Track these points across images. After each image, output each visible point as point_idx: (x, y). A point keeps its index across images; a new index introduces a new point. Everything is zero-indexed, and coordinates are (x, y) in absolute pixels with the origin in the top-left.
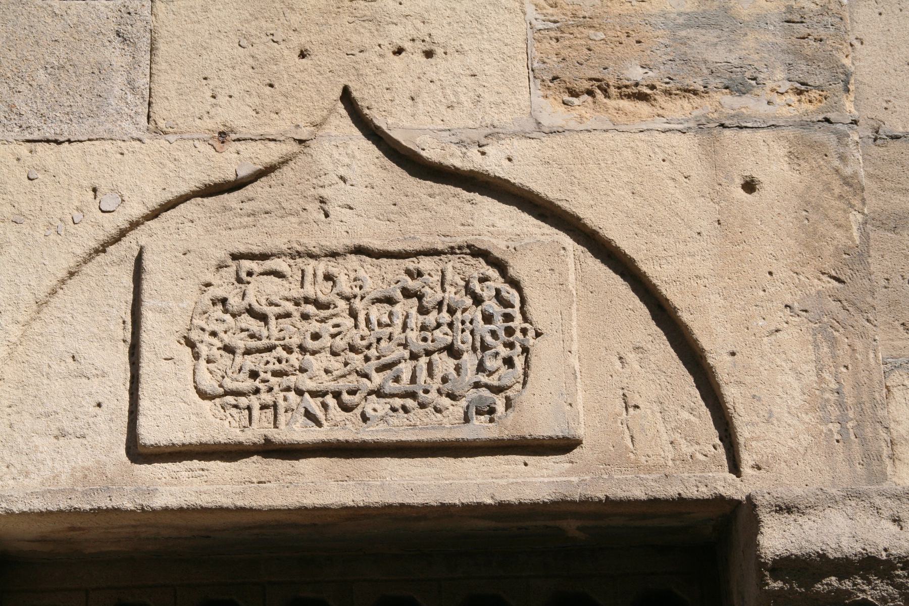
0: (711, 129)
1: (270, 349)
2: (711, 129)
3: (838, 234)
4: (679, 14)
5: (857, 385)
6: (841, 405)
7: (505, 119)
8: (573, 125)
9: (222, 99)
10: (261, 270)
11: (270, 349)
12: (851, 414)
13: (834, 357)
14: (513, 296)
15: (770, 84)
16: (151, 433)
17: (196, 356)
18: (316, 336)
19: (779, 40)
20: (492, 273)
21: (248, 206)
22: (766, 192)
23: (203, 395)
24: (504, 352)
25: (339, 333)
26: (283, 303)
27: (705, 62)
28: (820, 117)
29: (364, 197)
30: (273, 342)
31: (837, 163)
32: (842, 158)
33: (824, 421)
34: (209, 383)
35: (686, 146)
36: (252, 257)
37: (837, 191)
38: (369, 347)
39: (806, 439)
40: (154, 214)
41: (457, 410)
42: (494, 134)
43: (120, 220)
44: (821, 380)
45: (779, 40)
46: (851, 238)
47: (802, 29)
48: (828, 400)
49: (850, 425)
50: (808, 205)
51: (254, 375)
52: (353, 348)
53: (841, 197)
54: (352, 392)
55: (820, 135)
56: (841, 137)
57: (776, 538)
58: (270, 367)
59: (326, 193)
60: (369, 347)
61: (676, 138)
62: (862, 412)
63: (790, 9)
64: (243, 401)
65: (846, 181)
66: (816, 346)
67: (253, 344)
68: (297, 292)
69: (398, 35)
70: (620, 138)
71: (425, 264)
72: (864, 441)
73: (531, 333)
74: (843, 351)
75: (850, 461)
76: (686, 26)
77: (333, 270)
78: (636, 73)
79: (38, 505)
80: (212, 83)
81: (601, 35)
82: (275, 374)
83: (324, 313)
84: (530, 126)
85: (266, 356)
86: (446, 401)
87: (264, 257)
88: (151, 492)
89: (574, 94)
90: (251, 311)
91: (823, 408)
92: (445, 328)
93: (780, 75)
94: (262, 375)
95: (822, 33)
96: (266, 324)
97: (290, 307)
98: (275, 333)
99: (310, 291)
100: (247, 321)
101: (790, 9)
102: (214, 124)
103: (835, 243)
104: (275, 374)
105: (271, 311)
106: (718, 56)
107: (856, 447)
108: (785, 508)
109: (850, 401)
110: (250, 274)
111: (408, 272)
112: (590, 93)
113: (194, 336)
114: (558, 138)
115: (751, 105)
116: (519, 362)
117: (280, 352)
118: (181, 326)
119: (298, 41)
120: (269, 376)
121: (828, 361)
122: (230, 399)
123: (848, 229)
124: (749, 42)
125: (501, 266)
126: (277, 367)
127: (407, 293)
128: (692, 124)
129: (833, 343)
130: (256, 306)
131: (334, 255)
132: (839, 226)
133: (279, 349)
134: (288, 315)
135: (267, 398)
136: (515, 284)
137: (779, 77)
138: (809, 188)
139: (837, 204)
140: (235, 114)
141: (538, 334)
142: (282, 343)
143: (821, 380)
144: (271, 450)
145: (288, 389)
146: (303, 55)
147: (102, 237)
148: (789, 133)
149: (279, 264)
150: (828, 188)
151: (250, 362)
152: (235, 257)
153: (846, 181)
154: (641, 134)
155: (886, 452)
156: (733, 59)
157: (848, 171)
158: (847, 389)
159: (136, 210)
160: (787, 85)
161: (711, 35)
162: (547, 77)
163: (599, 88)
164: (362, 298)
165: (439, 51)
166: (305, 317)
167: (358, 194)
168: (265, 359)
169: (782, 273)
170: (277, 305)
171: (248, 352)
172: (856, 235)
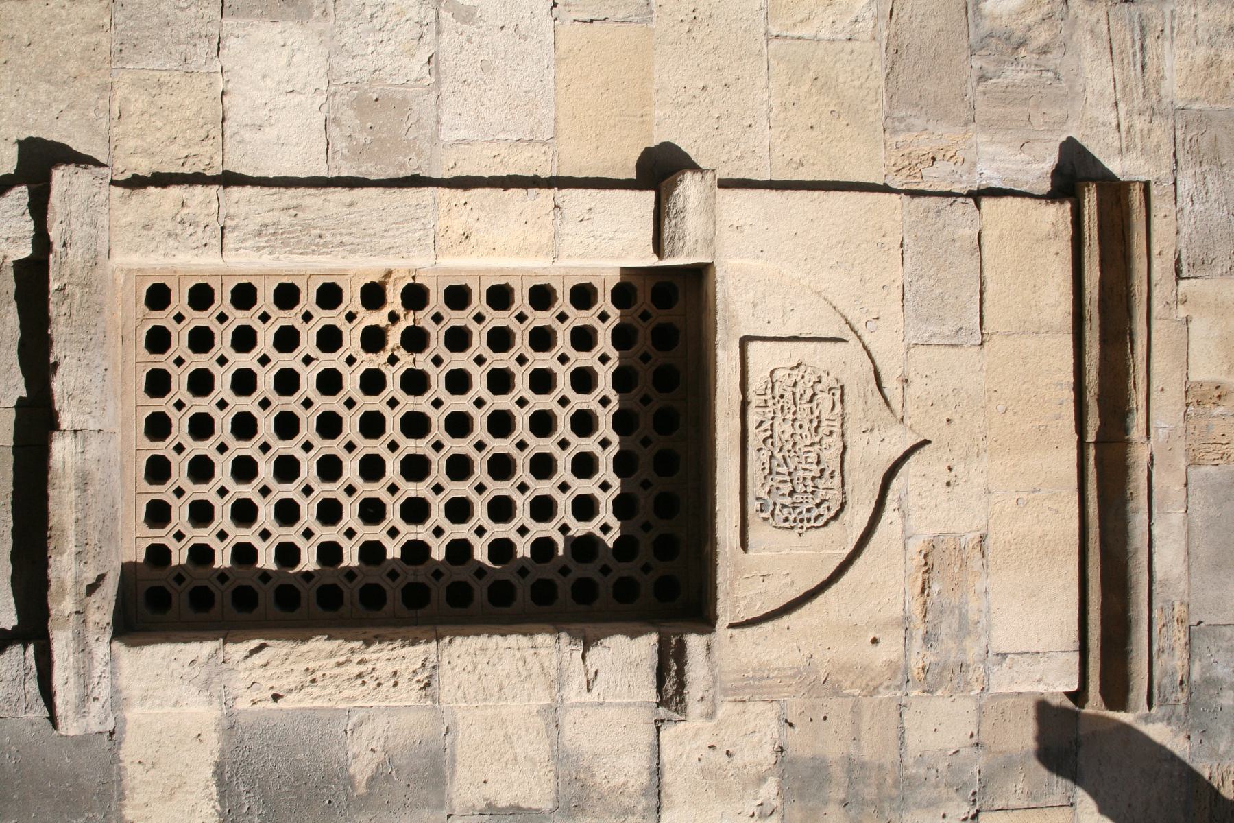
0: (905, 623)
1: (795, 404)
2: (905, 623)
3: (849, 683)
5: (771, 687)
6: (762, 678)
7: (913, 521)
8: (909, 555)
9: (925, 381)
11: (795, 404)
13: (786, 677)
14: (820, 522)
15: (928, 654)
16: (753, 347)
17: (792, 369)
18: (801, 426)
19: (952, 660)
20: (832, 513)
21: (869, 393)
22: (872, 649)
23: (772, 372)
24: (791, 518)
29: (873, 450)
31: (885, 684)
32: (888, 687)
33: (754, 670)
34: (778, 375)
35: (897, 611)
36: (842, 395)
40: (865, 348)
41: (763, 493)
42: (904, 516)
44: (774, 670)
45: (952, 660)
50: (864, 669)
51: (782, 396)
52: (794, 444)
54: (772, 444)
55: (900, 678)
56: (899, 687)
59: (876, 432)
61: (900, 606)
63: (968, 666)
64: (769, 391)
67: (798, 396)
68: (823, 417)
69: (959, 469)
70: (901, 578)
71: (837, 480)
72: (743, 688)
74: (788, 681)
75: (734, 680)
78: (935, 587)
79: (719, 295)
80: (934, 376)
82: (782, 407)
83: (813, 430)
84: (908, 534)
85: (791, 402)
86: (767, 489)
87: (842, 401)
89: (926, 556)
90: (814, 395)
93: (933, 659)
95: (955, 681)
97: (816, 414)
98: (803, 406)
99: (824, 423)
100: (809, 393)
101: (968, 666)
102: (911, 377)
104: (782, 407)
105: (814, 404)
106: (944, 630)
107: (740, 684)
108: (709, 648)
109: (763, 682)
111: (833, 472)
112: (926, 564)
113: (802, 368)
116: (786, 525)
118: (806, 361)
119: (956, 418)
121: (784, 673)
123: (851, 688)
124: (951, 645)
125: (835, 517)
127: (822, 471)
129: (793, 677)
131: (843, 435)
135: (770, 403)
136: (826, 524)
137: (931, 658)
143: (774, 670)
144: (745, 404)
146: (948, 420)
147: (853, 322)
148: (902, 662)
150: (872, 679)
151: (788, 395)
152: (842, 387)
153: (876, 688)
155: (738, 698)
156: (942, 636)
157: (881, 689)
158: (769, 682)
160: (927, 662)
161: (955, 625)
165: (950, 489)
167: (875, 447)
169: (829, 654)
171: (794, 394)
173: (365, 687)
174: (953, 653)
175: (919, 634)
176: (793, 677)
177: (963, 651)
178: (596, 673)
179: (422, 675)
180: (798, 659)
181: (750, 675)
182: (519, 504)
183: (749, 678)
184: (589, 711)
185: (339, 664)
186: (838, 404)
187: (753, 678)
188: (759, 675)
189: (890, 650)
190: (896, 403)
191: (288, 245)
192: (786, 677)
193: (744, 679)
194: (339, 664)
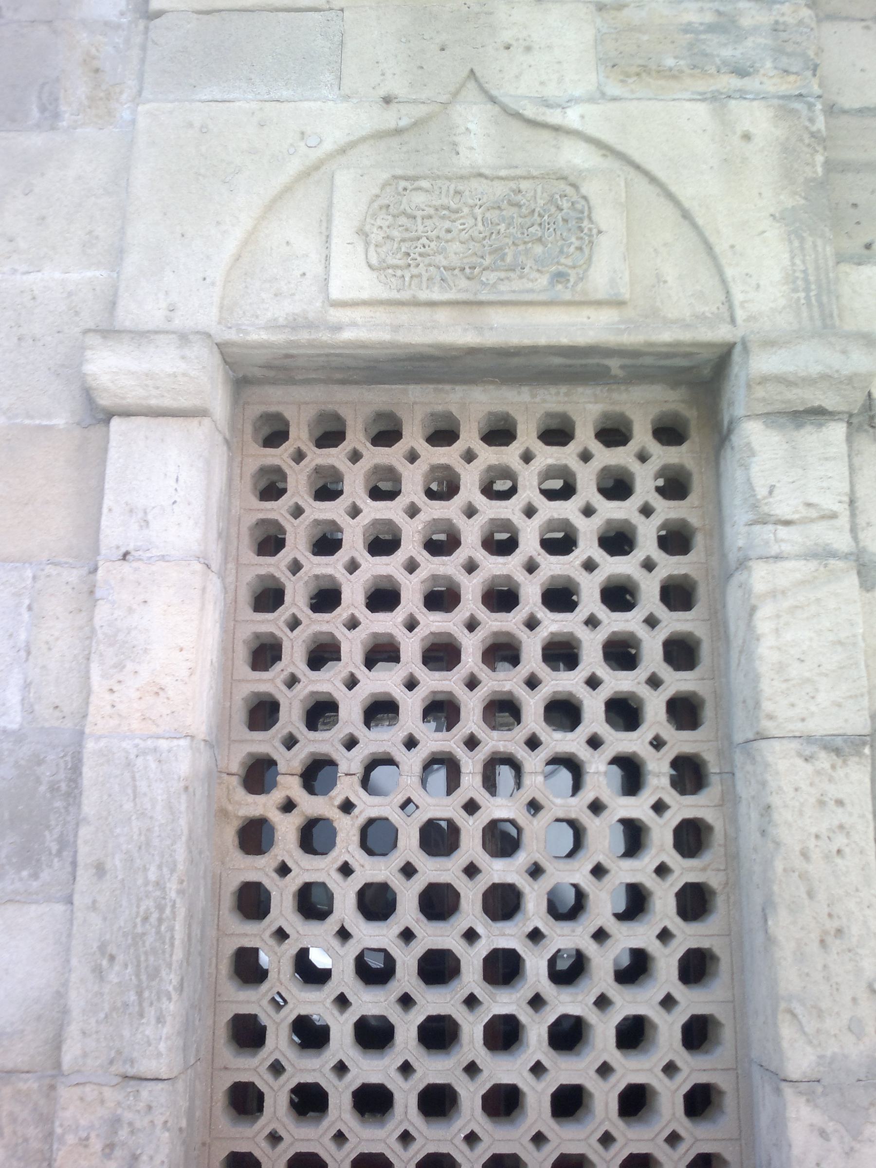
4: (701, 24)
5: (817, 268)
6: (806, 280)
10: (413, 187)
11: (418, 239)
12: (813, 287)
13: (802, 248)
15: (762, 71)
17: (367, 244)
18: (449, 231)
19: (769, 42)
20: (569, 190)
24: (577, 243)
25: (464, 230)
27: (718, 56)
28: (797, 93)
30: (420, 233)
31: (807, 124)
33: (795, 290)
36: (406, 178)
37: (807, 141)
38: (484, 239)
39: (782, 302)
40: (343, 151)
41: (544, 281)
43: (319, 153)
44: (793, 264)
46: (815, 172)
47: (784, 36)
48: (797, 278)
49: (812, 294)
50: (786, 150)
52: (472, 239)
53: (809, 145)
55: (797, 105)
56: (811, 106)
57: (762, 363)
59: (457, 139)
60: (484, 239)
62: (819, 287)
64: (399, 273)
65: (813, 135)
66: (790, 242)
67: (407, 235)
68: (438, 203)
69: (506, 36)
71: (524, 185)
72: (821, 305)
73: (595, 231)
74: (808, 245)
75: (811, 318)
76: (705, 32)
77: (460, 188)
78: (670, 62)
81: (645, 38)
82: (421, 255)
83: (454, 216)
85: (415, 244)
87: (415, 178)
88: (338, 328)
90: (404, 213)
91: (794, 282)
92: (536, 227)
93: (769, 64)
96: (416, 221)
97: (432, 211)
98: (421, 228)
99: (444, 201)
100: (403, 220)
101: (777, 22)
102: (382, 92)
103: (805, 175)
104: (421, 255)
105: (419, 214)
107: (816, 311)
109: (812, 278)
110: (405, 189)
112: (638, 74)
113: (367, 228)
114: (617, 104)
115: (750, 84)
116: (587, 250)
117: (424, 240)
120: (416, 256)
122: (390, 271)
124: (749, 43)
125: (574, 185)
127: (512, 204)
128: (709, 95)
129: (802, 240)
130: (409, 211)
131: (462, 177)
132: (808, 164)
134: (430, 217)
135: (415, 271)
138: (787, 139)
139: (806, 149)
140: (396, 86)
141: (600, 232)
143: (793, 264)
145: (430, 265)
146: (443, 49)
148: (776, 102)
149: (424, 184)
150: (801, 140)
152: (395, 177)
153: (813, 135)
154: (673, 103)
156: (738, 53)
157: (814, 129)
159: (328, 146)
160: (775, 72)
162: (610, 64)
163: (644, 71)
164: (480, 207)
166: (443, 218)
170: (423, 210)
171: (403, 240)
172: (820, 170)
173: (847, 850)
174: (761, 41)
175: (735, 82)
176: (802, 240)
177: (755, 30)
178: (809, 505)
179: (824, 760)
180: (774, 232)
181: (802, 295)
182: (554, 628)
183: (808, 298)
184: (861, 520)
185: (811, 894)
186: (417, 184)
187: (807, 290)
188: (800, 283)
189: (757, 119)
190: (421, 111)
191: (157, 970)
192: (802, 248)
193: (809, 304)
194: (811, 894)
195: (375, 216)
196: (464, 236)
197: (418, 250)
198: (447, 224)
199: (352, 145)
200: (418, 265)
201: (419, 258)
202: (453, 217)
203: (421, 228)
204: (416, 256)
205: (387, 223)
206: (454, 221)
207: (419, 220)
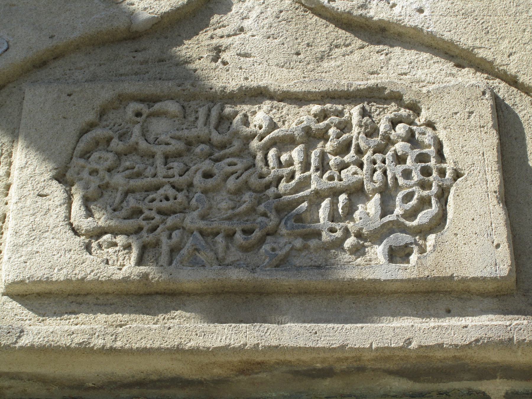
11: (157, 188)
18: (208, 175)
21: (140, 56)
26: (173, 142)
30: (160, 179)
40: (40, 64)
58: (156, 205)
94: (147, 213)
105: (159, 150)
110: (138, 114)
120: (153, 214)
126: (165, 204)
133: (167, 187)
142: (171, 180)
168: (151, 197)
170: (167, 144)
186: (157, 106)
195: (86, 155)
196: (231, 183)
197: (156, 205)
198: (206, 165)
199: (57, 55)
200: (153, 229)
201: (158, 217)
202: (217, 155)
203: (161, 170)
204: (153, 214)
205: (108, 164)
206: (217, 160)
207: (159, 161)
